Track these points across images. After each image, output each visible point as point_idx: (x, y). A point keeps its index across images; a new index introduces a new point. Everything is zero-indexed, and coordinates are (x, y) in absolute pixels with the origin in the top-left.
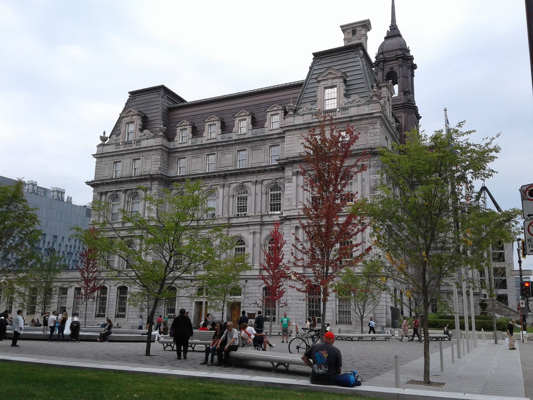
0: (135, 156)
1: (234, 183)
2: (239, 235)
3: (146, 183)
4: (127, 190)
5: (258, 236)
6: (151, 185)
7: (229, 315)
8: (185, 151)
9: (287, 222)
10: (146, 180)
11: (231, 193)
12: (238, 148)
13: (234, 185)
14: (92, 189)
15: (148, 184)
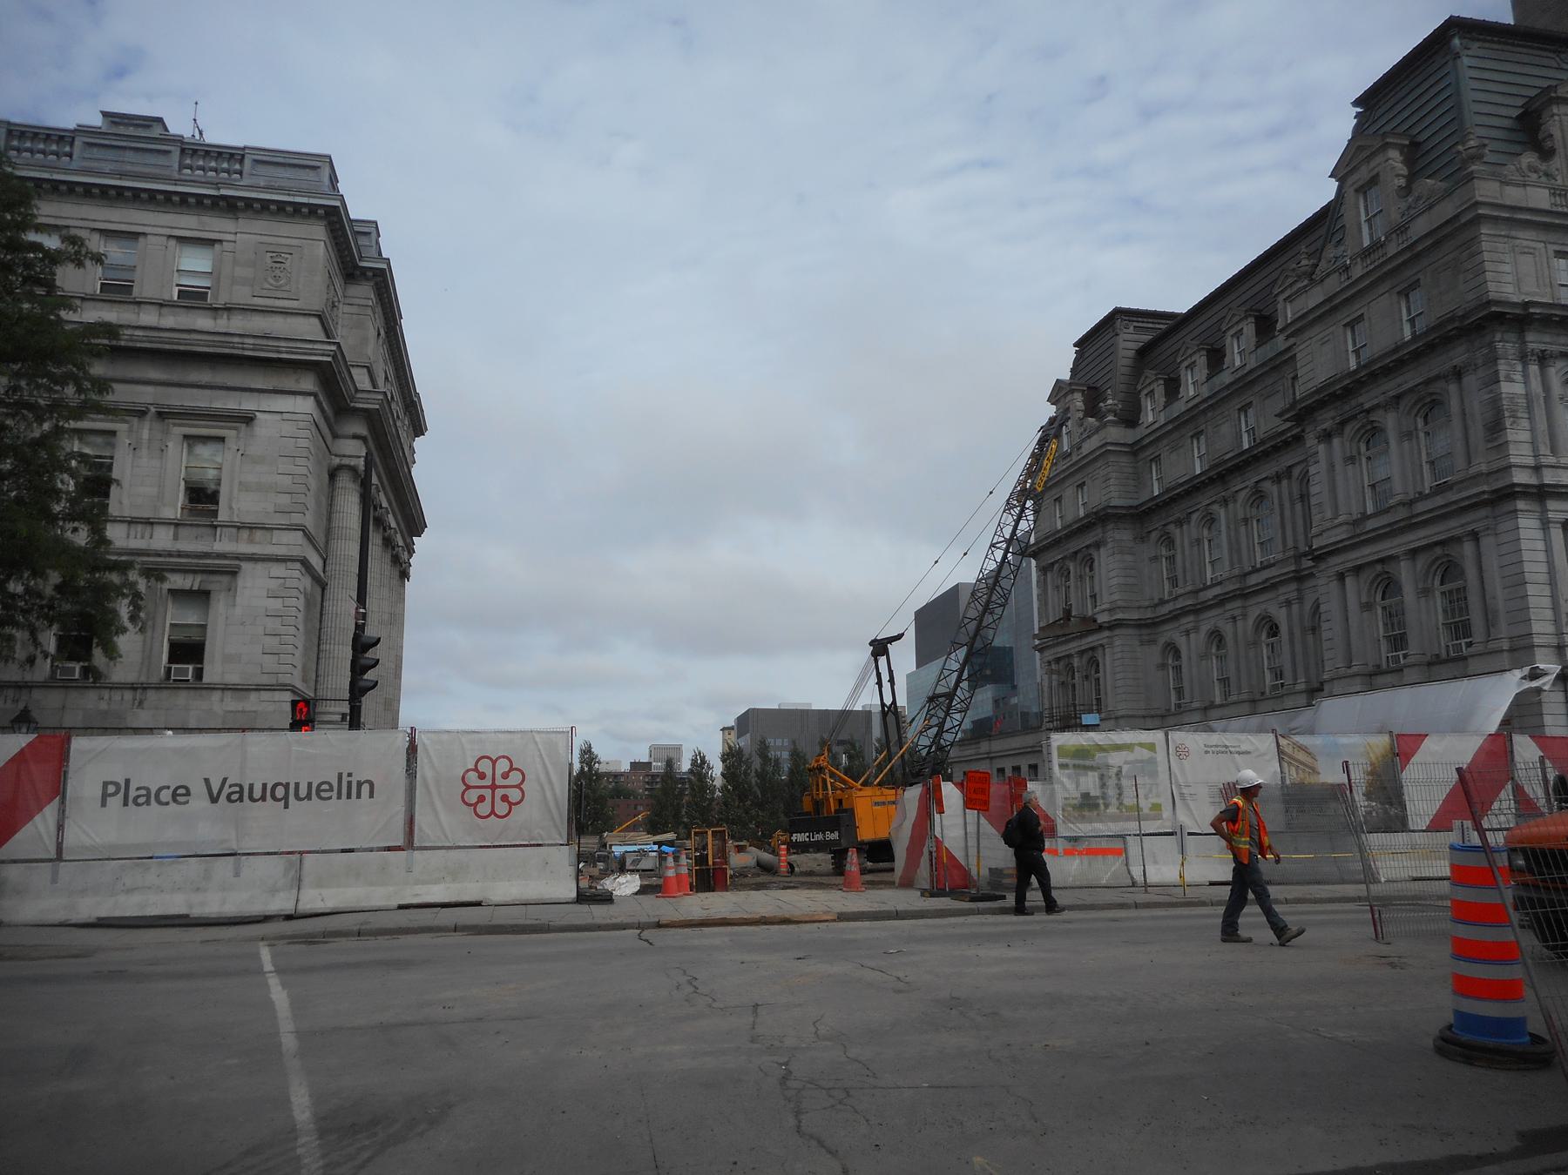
0: (1078, 478)
1: (1242, 485)
4: (1076, 553)
5: (1295, 607)
8: (1158, 439)
9: (1323, 566)
11: (1241, 515)
12: (1237, 403)
13: (1243, 494)
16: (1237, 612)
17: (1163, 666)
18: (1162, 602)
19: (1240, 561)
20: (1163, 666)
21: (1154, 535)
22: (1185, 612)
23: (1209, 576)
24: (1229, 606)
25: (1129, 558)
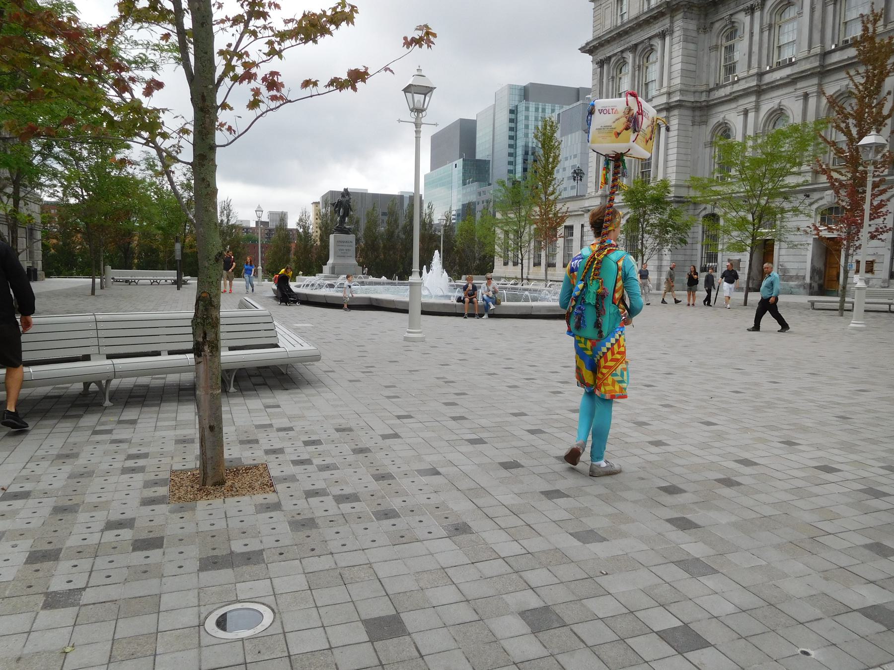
2: (843, 89)
3: (663, 22)
6: (672, 22)
7: (820, 265)
10: (661, 14)
14: (591, 58)
15: (663, 24)
16: (809, 90)
17: (712, 144)
18: (718, 87)
19: (822, 41)
20: (712, 144)
21: (718, 26)
22: (746, 93)
23: (775, 61)
24: (800, 85)
25: (692, 46)
